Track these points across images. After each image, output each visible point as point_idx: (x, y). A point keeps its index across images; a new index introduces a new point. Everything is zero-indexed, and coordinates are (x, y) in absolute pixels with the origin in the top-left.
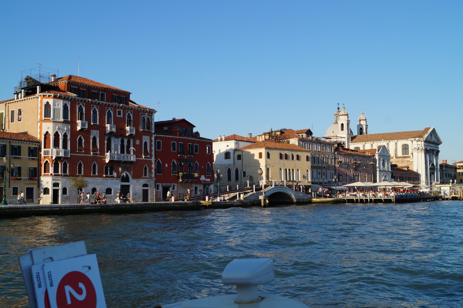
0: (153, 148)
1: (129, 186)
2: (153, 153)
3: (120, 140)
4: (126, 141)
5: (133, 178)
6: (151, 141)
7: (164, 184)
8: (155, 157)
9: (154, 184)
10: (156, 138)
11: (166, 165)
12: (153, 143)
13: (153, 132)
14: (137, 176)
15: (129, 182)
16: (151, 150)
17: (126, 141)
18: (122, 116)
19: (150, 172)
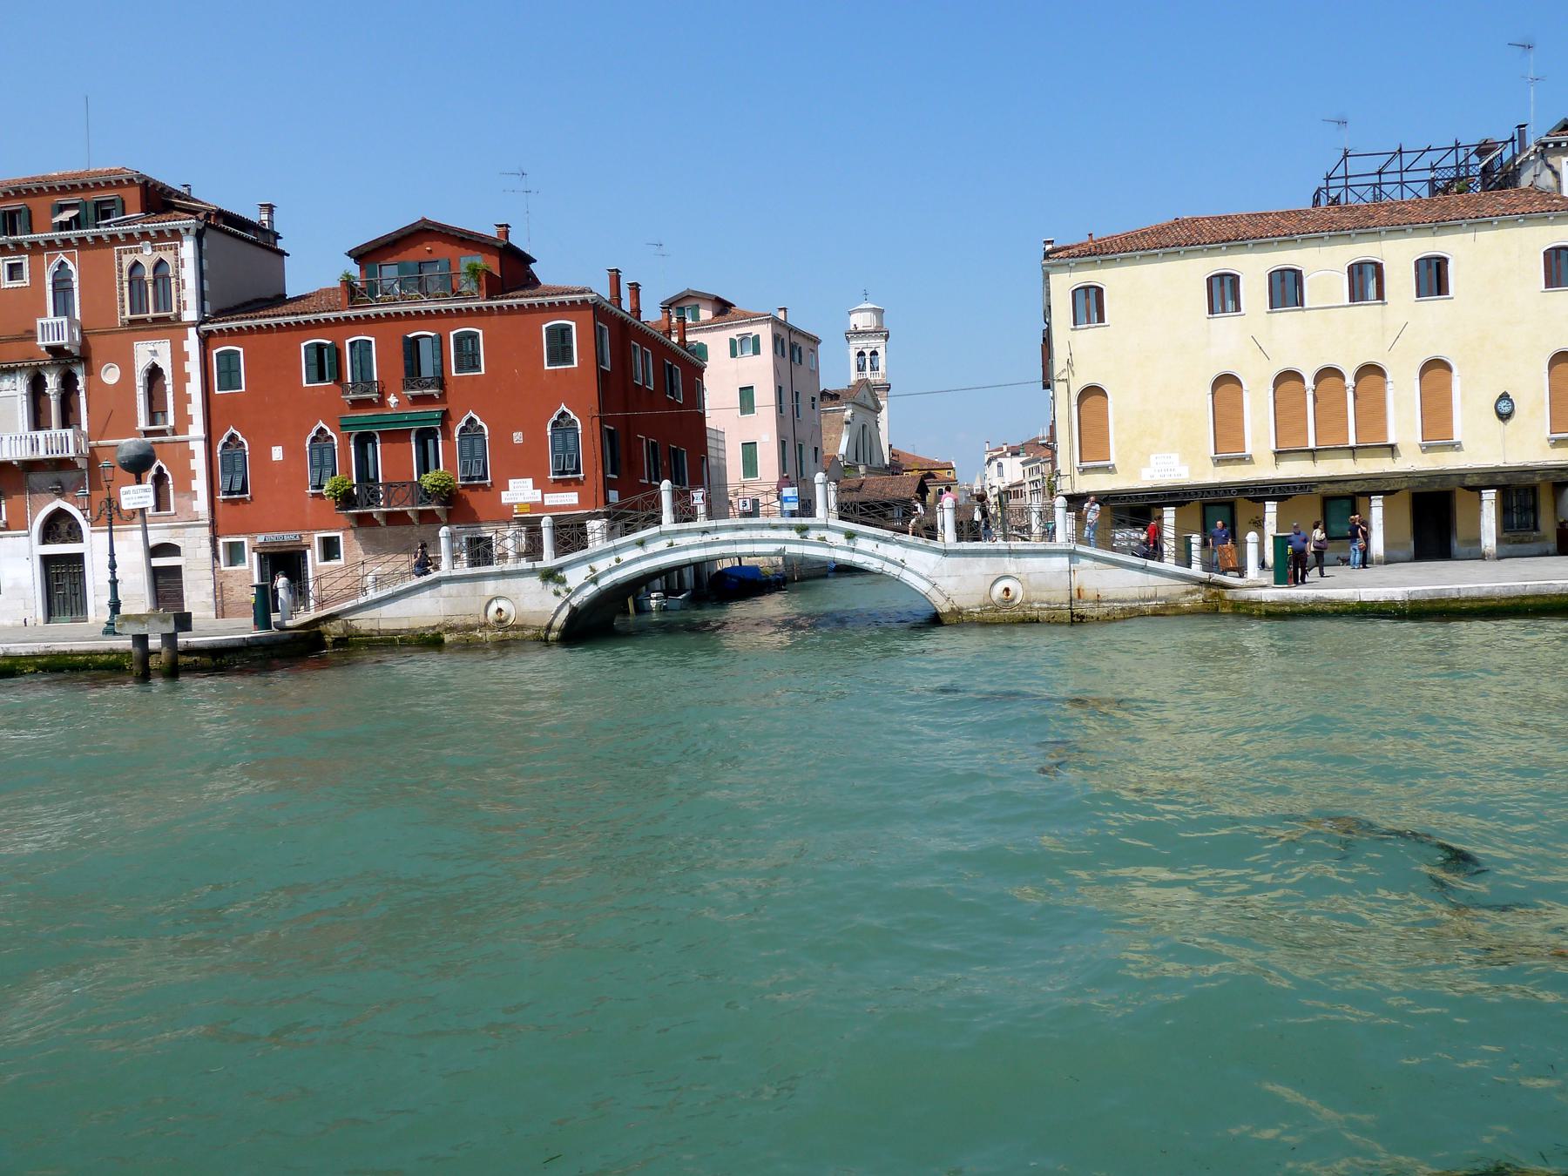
0: (194, 388)
1: (78, 558)
2: (196, 409)
4: (52, 382)
6: (179, 357)
9: (207, 543)
10: (205, 340)
11: (277, 453)
12: (193, 367)
13: (190, 315)
16: (182, 399)
17: (52, 382)
19: (185, 488)
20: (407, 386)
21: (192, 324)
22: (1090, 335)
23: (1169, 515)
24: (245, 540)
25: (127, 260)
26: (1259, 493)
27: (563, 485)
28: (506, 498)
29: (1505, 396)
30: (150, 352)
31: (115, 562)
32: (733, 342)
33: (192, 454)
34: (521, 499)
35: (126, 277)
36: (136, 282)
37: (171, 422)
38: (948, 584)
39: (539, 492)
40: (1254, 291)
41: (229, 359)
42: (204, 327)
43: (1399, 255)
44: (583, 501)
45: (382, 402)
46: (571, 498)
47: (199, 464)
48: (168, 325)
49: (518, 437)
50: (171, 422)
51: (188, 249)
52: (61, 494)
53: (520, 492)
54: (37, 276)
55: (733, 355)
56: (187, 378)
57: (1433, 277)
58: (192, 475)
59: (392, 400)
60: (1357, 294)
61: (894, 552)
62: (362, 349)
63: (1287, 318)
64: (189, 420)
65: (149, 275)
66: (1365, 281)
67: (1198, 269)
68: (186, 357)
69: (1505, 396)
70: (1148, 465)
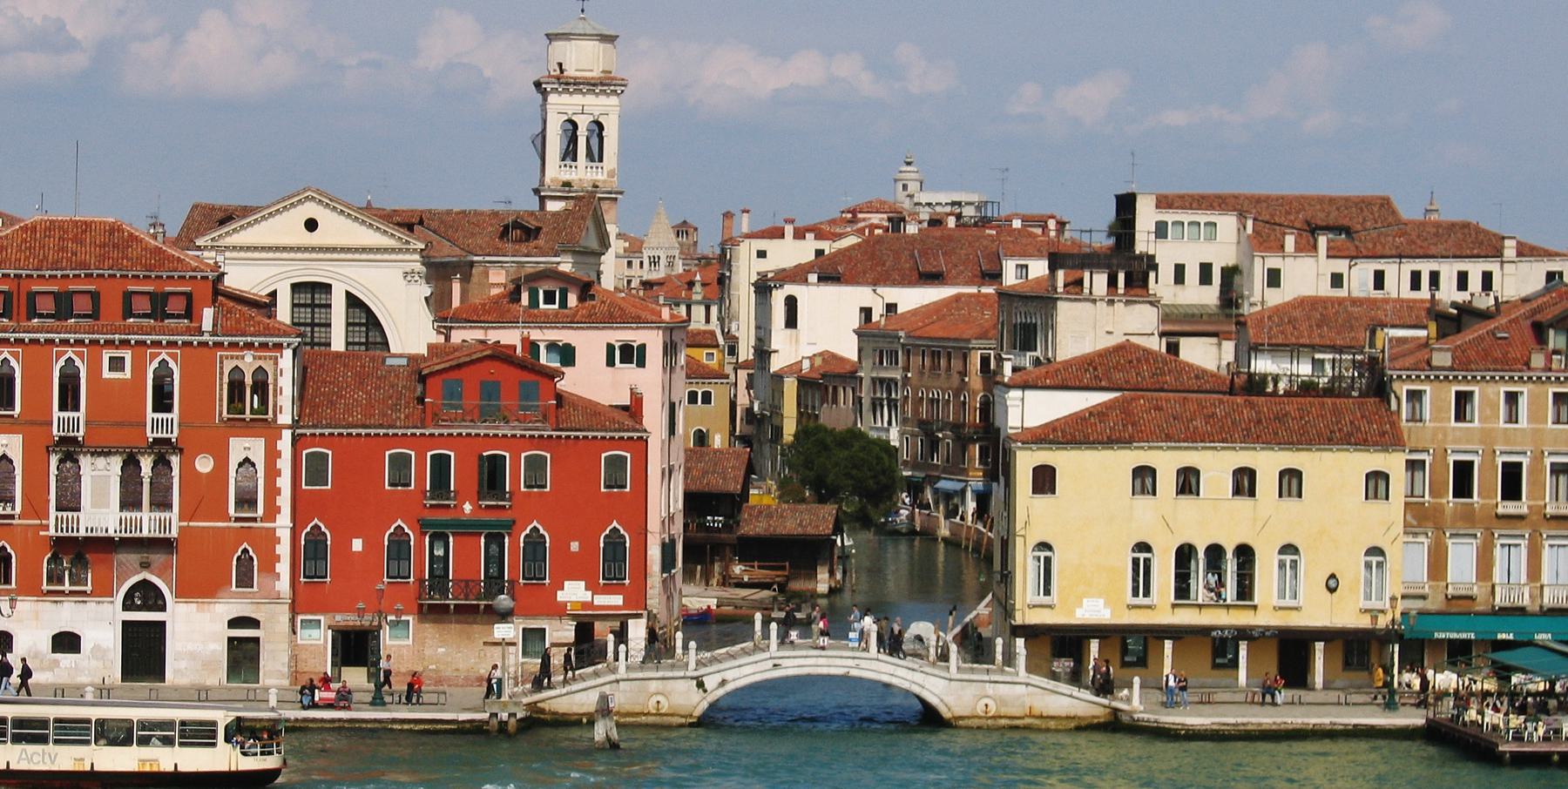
0: (284, 482)
1: (163, 624)
2: (284, 501)
3: (116, 463)
4: (146, 464)
5: (182, 593)
6: (272, 455)
7: (338, 617)
8: (294, 518)
10: (295, 440)
11: (357, 545)
12: (285, 464)
13: (285, 418)
14: (198, 588)
15: (163, 608)
16: (272, 492)
17: (146, 464)
18: (128, 374)
20: (481, 497)
21: (289, 427)
22: (1043, 500)
23: (1094, 645)
24: (322, 618)
25: (228, 366)
26: (1159, 633)
27: (607, 590)
28: (561, 596)
29: (1333, 576)
30: (242, 447)
31: (195, 633)
32: (610, 349)
33: (278, 541)
34: (574, 599)
35: (226, 380)
36: (236, 388)
37: (260, 511)
38: (949, 700)
39: (589, 593)
40: (1167, 481)
41: (317, 461)
42: (299, 431)
43: (1268, 463)
44: (626, 605)
45: (459, 508)
46: (617, 600)
47: (284, 549)
48: (264, 426)
49: (575, 546)
50: (260, 511)
51: (286, 360)
52: (145, 566)
53: (574, 592)
54: (139, 369)
55: (610, 362)
56: (279, 473)
57: (1291, 481)
58: (278, 559)
59: (468, 507)
60: (1237, 491)
61: (918, 677)
62: (441, 464)
63: (1186, 501)
64: (278, 510)
65: (249, 380)
66: (1245, 483)
67: (1129, 458)
68: (279, 454)
69: (1333, 576)
70: (1081, 605)
